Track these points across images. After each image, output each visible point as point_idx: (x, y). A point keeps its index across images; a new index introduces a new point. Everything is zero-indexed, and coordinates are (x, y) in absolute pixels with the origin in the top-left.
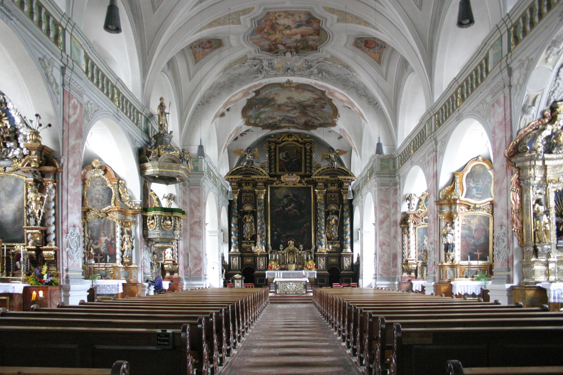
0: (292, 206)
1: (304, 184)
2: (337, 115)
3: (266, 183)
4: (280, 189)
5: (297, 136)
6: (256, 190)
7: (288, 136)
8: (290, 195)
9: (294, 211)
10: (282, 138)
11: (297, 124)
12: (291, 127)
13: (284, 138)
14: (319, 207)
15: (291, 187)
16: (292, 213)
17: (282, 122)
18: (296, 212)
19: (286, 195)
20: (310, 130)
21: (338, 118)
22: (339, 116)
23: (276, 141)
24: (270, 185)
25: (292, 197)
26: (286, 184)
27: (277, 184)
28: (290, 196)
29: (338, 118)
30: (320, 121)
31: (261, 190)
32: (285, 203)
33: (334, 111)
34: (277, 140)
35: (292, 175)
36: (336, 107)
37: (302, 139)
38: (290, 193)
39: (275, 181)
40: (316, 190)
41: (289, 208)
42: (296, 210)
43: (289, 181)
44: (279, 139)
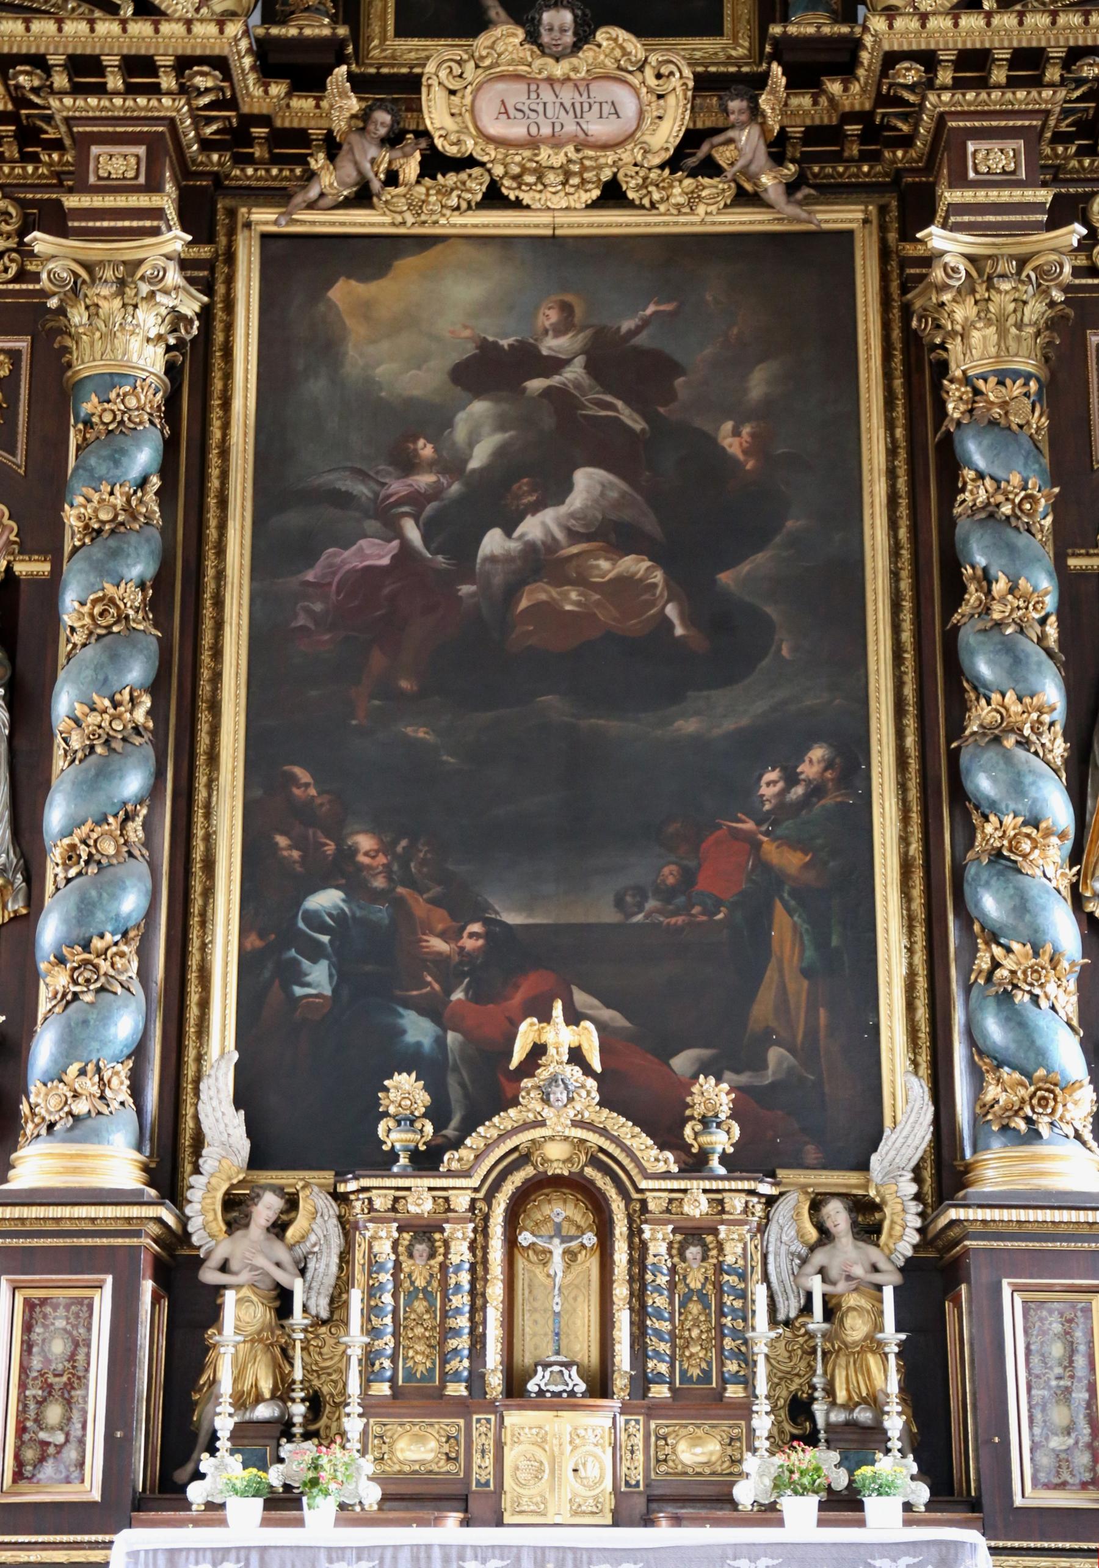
0: (577, 500)
1: (746, 198)
3: (217, 179)
4: (408, 265)
6: (41, 242)
8: (551, 345)
9: (605, 567)
14: (975, 494)
15: (554, 241)
16: (572, 599)
18: (625, 583)
19: (487, 350)
24: (265, 218)
25: (574, 373)
26: (494, 198)
27: (362, 197)
28: (555, 365)
31: (128, 250)
32: (479, 458)
35: (583, 36)
38: (550, 316)
39: (332, 147)
40: (936, 237)
41: (533, 527)
42: (635, 565)
43: (533, 143)
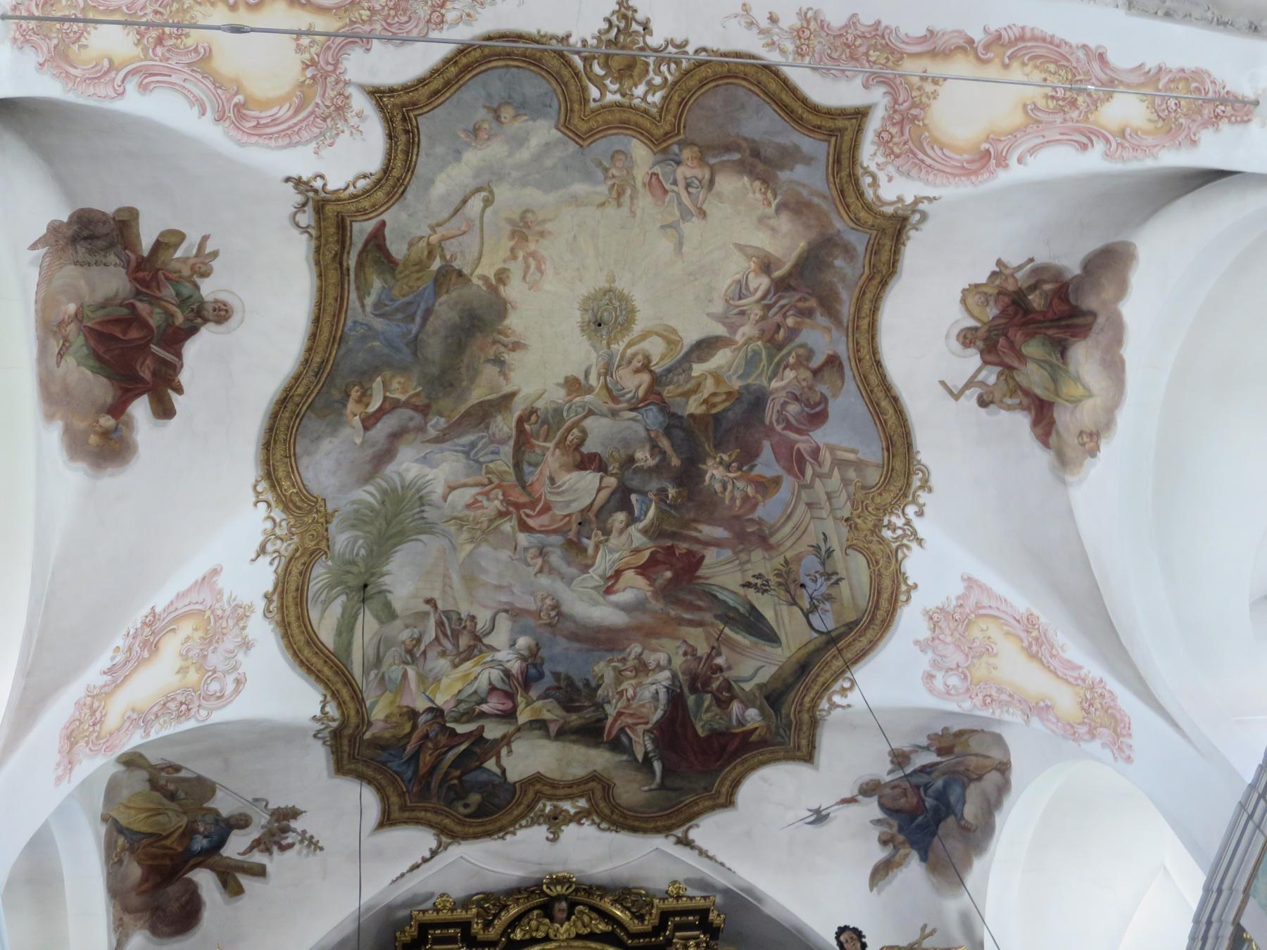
2: (908, 475)
5: (606, 904)
7: (547, 909)
10: (506, 917)
11: (617, 745)
12: (572, 788)
13: (514, 923)
17: (523, 717)
20: (691, 817)
21: (923, 497)
22: (925, 486)
23: (465, 926)
29: (923, 497)
30: (771, 637)
33: (890, 445)
34: (477, 928)
36: (895, 401)
37: (641, 918)
44: (488, 925)
